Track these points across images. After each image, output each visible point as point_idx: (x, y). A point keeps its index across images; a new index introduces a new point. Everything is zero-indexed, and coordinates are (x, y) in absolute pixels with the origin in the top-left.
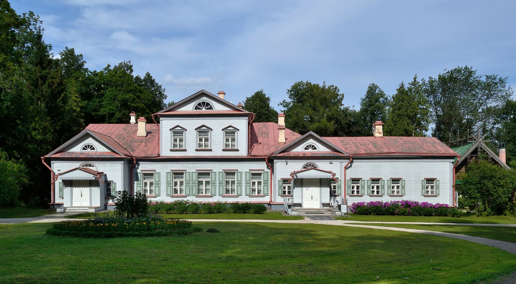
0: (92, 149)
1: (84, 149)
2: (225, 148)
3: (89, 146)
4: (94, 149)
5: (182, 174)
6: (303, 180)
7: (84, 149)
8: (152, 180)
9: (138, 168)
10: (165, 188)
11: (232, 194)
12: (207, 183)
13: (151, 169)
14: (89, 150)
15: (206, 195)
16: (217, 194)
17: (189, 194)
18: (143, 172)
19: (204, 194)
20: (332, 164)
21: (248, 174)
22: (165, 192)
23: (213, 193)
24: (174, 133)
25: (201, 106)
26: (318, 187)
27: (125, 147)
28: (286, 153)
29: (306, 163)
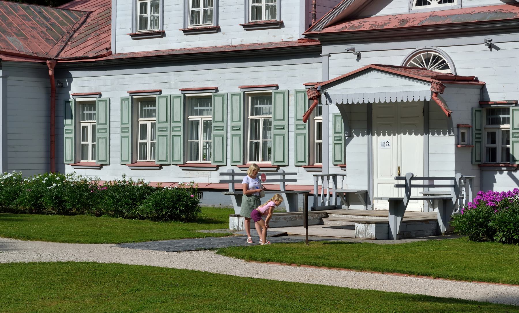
2: (250, 21)
5: (151, 102)
6: (374, 112)
8: (94, 122)
9: (69, 88)
10: (118, 142)
11: (207, 162)
12: (207, 125)
13: (93, 91)
15: (207, 162)
17: (166, 161)
18: (77, 100)
19: (200, 161)
20: (498, 49)
22: (119, 154)
23: (218, 158)
26: (363, 135)
27: (76, 34)
28: (356, 23)
29: (411, 51)
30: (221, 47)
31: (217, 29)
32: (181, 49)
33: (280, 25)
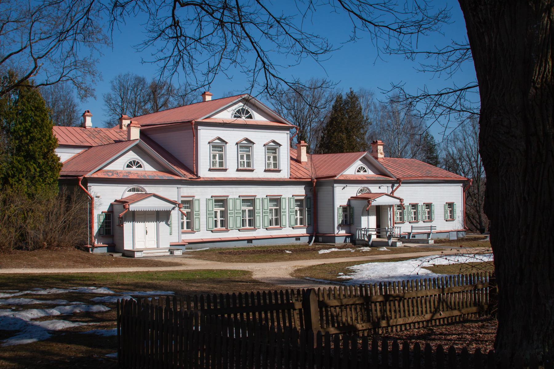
0: (138, 167)
1: (128, 166)
3: (134, 162)
4: (140, 166)
7: (128, 166)
13: (190, 195)
14: (134, 167)
16: (288, 225)
21: (292, 201)
24: (214, 147)
25: (240, 114)
30: (234, 178)
31: (252, 171)
32: (237, 178)
33: (279, 171)
